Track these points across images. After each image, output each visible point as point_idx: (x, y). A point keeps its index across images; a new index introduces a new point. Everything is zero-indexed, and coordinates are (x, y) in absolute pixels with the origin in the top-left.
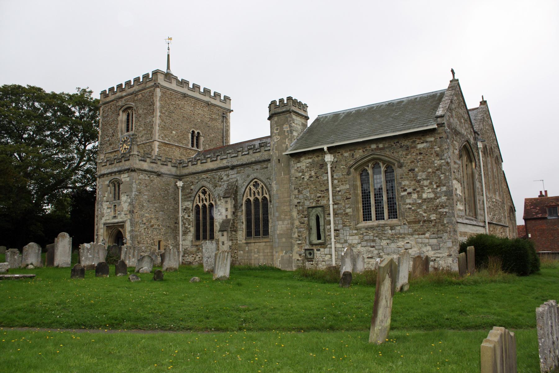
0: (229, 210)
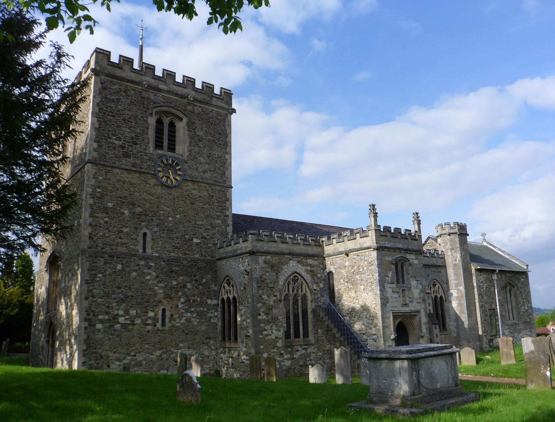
0: (431, 305)
